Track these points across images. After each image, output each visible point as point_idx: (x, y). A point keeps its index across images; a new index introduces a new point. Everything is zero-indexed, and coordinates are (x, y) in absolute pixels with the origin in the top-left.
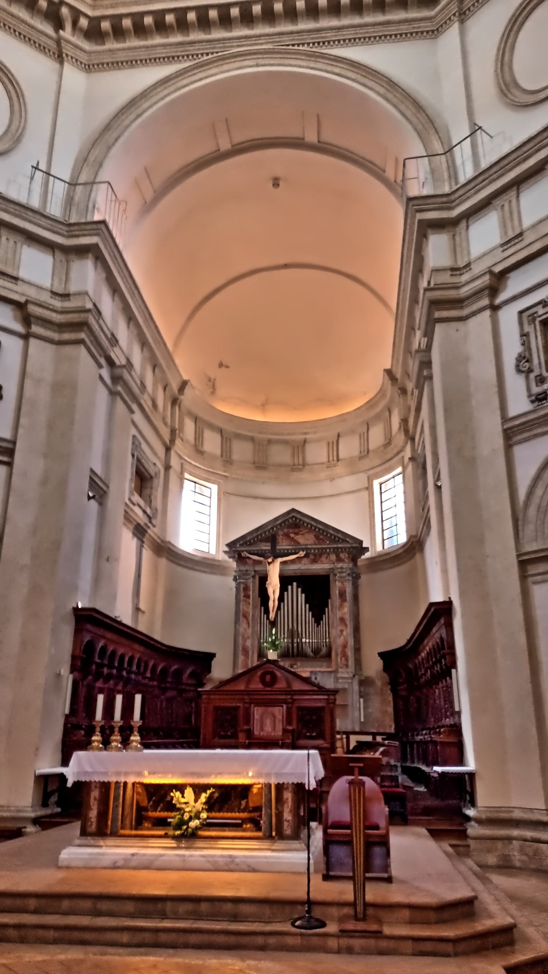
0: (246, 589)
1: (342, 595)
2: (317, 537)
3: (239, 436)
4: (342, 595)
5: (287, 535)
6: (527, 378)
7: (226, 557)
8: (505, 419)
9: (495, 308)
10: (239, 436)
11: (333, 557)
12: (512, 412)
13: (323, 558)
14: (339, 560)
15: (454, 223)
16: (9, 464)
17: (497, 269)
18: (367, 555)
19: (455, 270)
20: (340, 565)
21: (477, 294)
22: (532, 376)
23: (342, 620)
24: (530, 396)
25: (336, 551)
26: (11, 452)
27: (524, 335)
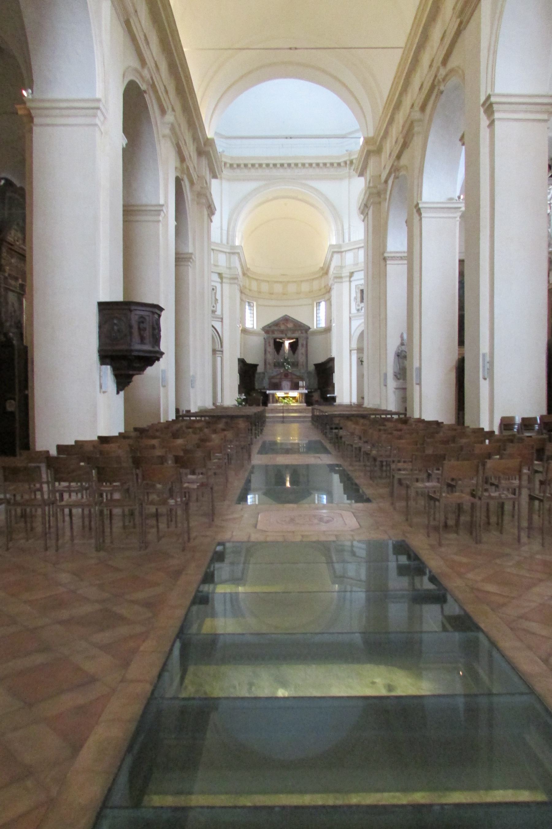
0: (269, 343)
1: (302, 345)
2: (294, 325)
3: (263, 281)
4: (302, 345)
5: (283, 324)
6: (356, 304)
7: (261, 330)
8: (350, 313)
9: (350, 281)
10: (263, 281)
11: (300, 332)
12: (352, 312)
13: (297, 332)
14: (302, 333)
15: (342, 252)
16: (222, 321)
17: (352, 271)
18: (311, 330)
19: (341, 267)
20: (302, 335)
21: (346, 276)
22: (357, 304)
23: (302, 354)
24: (356, 308)
25: (301, 330)
26: (222, 319)
27: (356, 292)
